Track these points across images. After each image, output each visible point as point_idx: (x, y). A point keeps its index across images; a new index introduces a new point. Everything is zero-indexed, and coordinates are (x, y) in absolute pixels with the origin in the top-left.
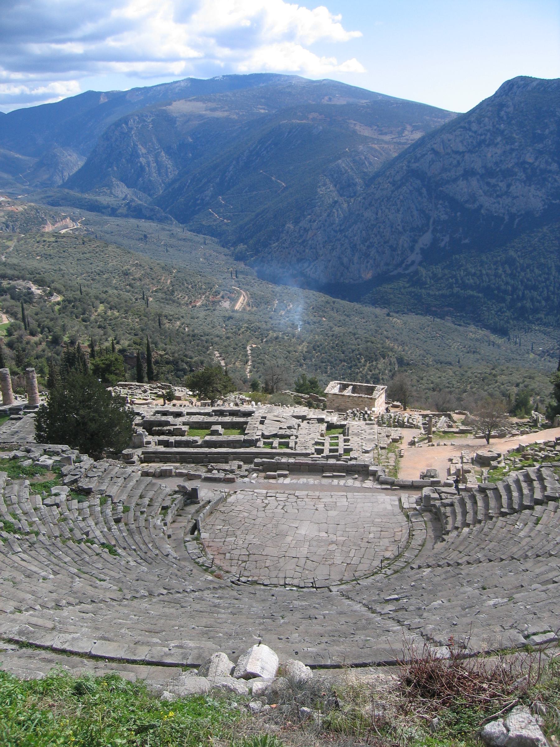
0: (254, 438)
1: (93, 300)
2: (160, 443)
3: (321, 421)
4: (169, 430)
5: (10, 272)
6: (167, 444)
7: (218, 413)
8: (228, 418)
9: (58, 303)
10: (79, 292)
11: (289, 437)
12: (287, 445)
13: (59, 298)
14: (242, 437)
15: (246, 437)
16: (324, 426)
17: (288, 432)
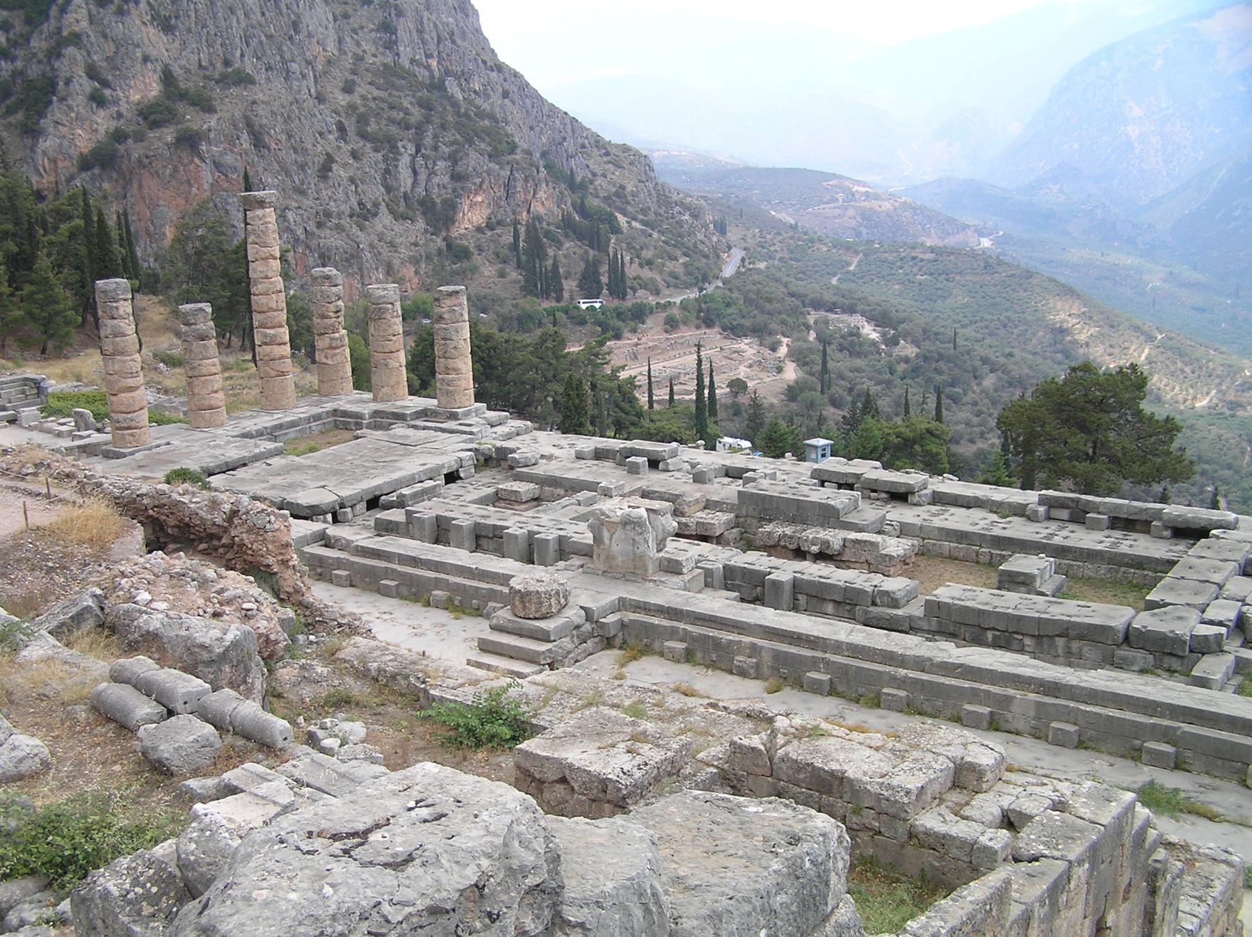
0: (1182, 630)
1: (978, 363)
2: (732, 579)
4: (826, 543)
5: (828, 297)
6: (755, 589)
7: (1065, 514)
8: (1099, 535)
9: (907, 360)
10: (952, 345)
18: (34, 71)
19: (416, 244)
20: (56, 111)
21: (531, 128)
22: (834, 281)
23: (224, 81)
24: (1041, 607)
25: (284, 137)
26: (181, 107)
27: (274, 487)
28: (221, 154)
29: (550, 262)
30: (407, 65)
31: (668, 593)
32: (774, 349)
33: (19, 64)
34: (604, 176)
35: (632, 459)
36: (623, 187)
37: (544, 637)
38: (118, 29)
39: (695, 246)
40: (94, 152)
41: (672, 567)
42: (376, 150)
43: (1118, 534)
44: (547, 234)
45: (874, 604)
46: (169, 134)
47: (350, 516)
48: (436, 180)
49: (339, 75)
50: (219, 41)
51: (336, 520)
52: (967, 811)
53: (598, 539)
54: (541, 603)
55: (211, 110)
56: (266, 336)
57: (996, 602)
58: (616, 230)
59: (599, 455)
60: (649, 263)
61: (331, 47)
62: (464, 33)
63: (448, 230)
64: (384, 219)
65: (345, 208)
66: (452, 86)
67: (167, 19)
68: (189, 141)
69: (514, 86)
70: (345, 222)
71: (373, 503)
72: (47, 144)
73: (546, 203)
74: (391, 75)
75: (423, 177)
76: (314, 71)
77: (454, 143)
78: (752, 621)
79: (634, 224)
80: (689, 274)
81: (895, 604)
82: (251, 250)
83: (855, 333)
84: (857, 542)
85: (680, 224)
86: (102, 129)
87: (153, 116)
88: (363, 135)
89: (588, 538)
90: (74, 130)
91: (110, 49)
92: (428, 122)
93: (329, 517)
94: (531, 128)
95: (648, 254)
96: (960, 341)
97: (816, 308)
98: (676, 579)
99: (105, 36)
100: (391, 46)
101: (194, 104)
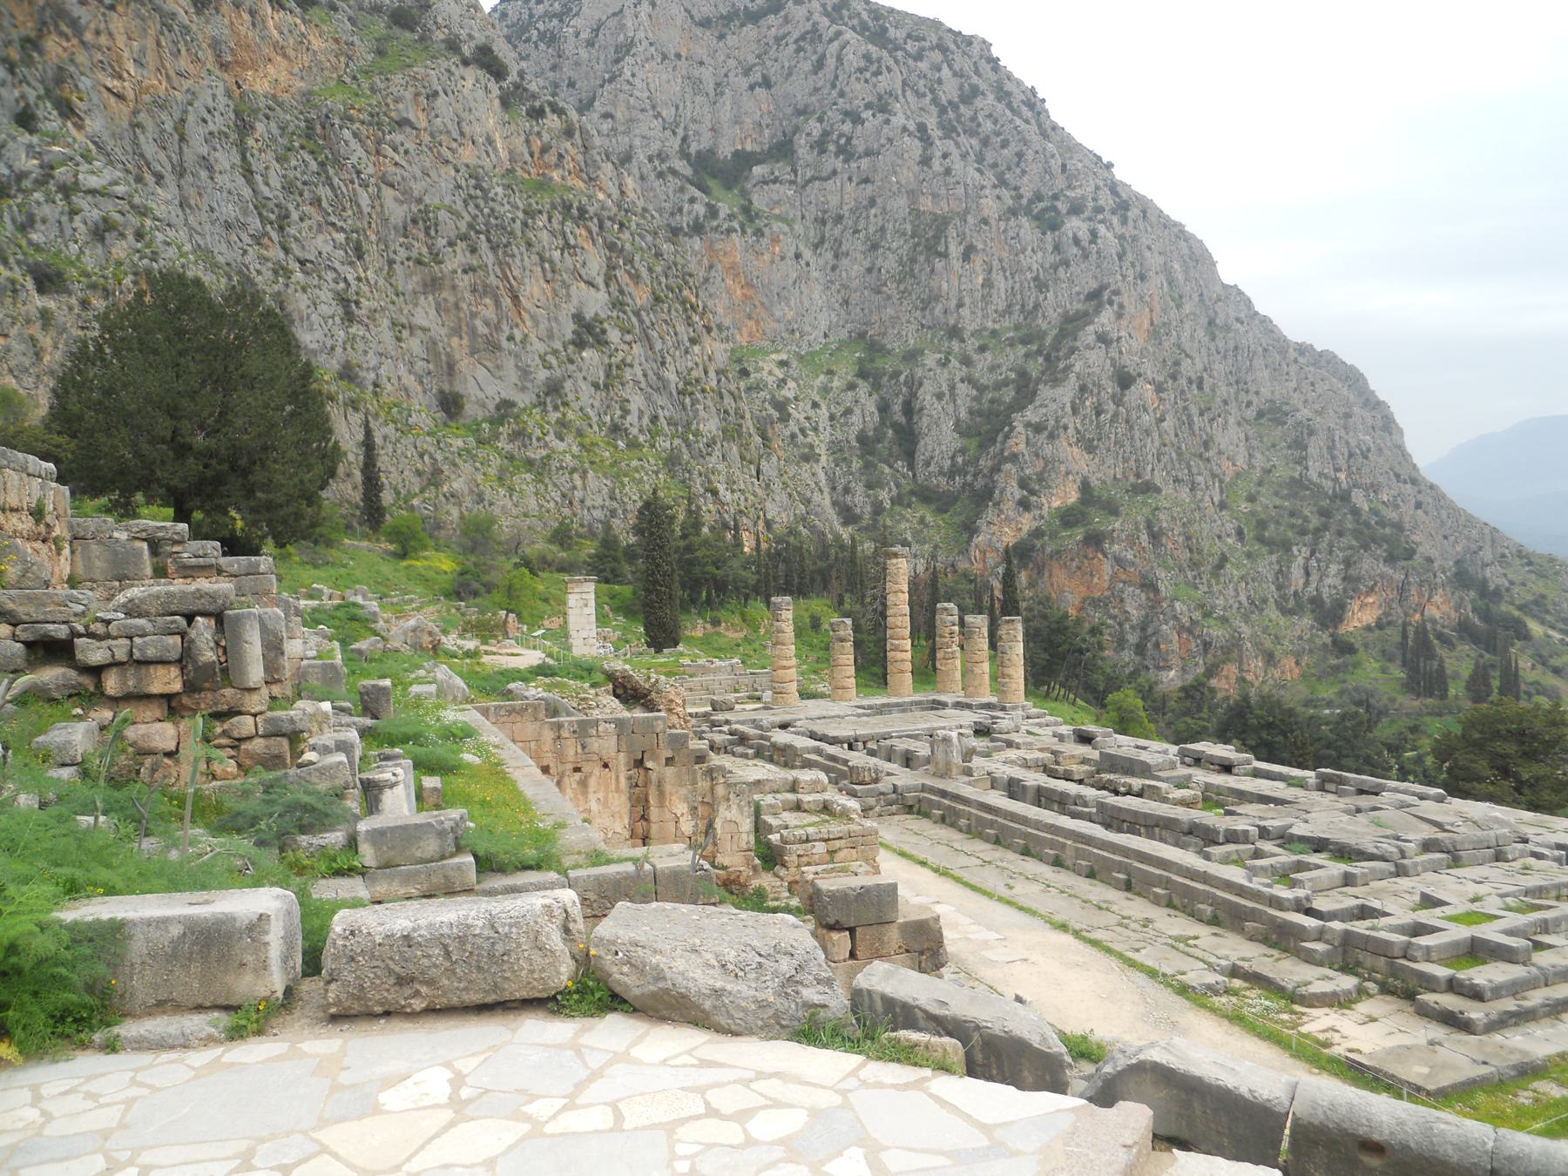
7: (1332, 787)
18: (979, 483)
20: (990, 514)
23: (1136, 490)
26: (1092, 510)
33: (969, 478)
38: (1048, 450)
41: (968, 772)
46: (1079, 534)
51: (851, 748)
68: (1095, 540)
69: (1427, 495)
72: (980, 539)
76: (1221, 481)
82: (888, 585)
86: (1026, 528)
87: (1069, 518)
90: (1004, 529)
91: (1040, 464)
94: (1445, 537)
98: (967, 779)
99: (1037, 455)
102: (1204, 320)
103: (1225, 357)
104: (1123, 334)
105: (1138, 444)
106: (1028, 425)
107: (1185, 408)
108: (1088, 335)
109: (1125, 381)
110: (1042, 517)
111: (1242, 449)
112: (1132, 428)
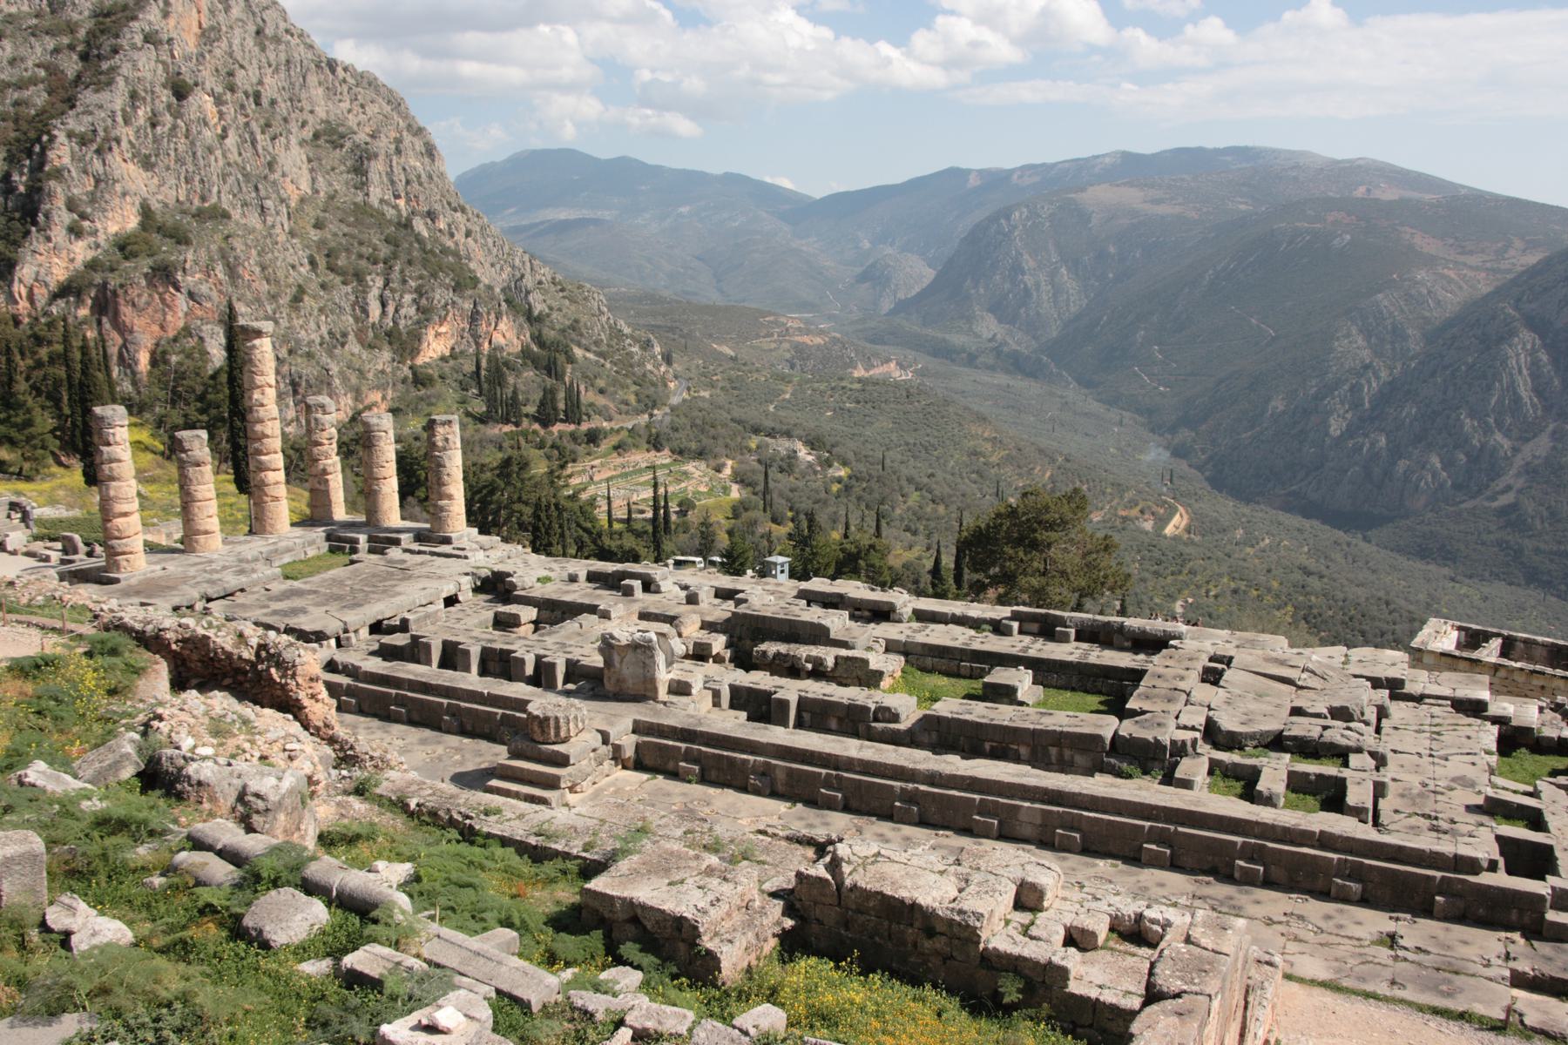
0: (1165, 740)
1: (904, 483)
3: (1474, 709)
4: (818, 662)
5: (768, 423)
6: (761, 707)
7: (1035, 627)
9: (839, 480)
11: (1341, 754)
12: (1332, 797)
13: (843, 473)
14: (1108, 726)
15: (1128, 728)
16: (1489, 735)
17: (1338, 734)
19: (383, 372)
20: (36, 241)
21: (492, 265)
22: (771, 408)
24: (1034, 717)
25: (257, 270)
26: (156, 238)
27: (275, 613)
28: (196, 284)
29: (509, 391)
30: (376, 204)
31: (679, 713)
32: (718, 470)
34: (560, 310)
35: (627, 582)
36: (577, 321)
37: (563, 761)
39: (644, 375)
40: (70, 280)
41: (680, 689)
42: (345, 283)
43: (1085, 646)
44: (506, 364)
45: (876, 720)
47: (354, 640)
48: (403, 312)
49: (312, 213)
50: (197, 178)
52: (1034, 931)
53: (608, 662)
54: (558, 728)
55: (187, 242)
56: (260, 462)
57: (991, 714)
58: (571, 359)
59: (593, 577)
60: (602, 391)
61: (305, 187)
62: (430, 177)
63: (412, 359)
64: (353, 346)
65: (315, 337)
66: (419, 225)
67: (147, 157)
70: (316, 348)
71: (376, 628)
73: (507, 335)
74: (362, 213)
75: (391, 309)
76: (288, 207)
77: (421, 277)
78: (764, 740)
79: (590, 356)
80: (639, 401)
81: (895, 718)
83: (793, 455)
84: (848, 659)
85: (630, 355)
88: (331, 268)
89: (597, 661)
92: (395, 256)
93: (333, 642)
95: (601, 383)
96: (888, 461)
97: (756, 430)
100: (363, 186)
101: (171, 237)
102: (252, 28)
103: (277, 70)
104: (174, 35)
105: (202, 162)
106: (70, 135)
107: (247, 124)
108: (134, 33)
109: (181, 91)
110: (98, 246)
111: (305, 172)
112: (193, 144)
